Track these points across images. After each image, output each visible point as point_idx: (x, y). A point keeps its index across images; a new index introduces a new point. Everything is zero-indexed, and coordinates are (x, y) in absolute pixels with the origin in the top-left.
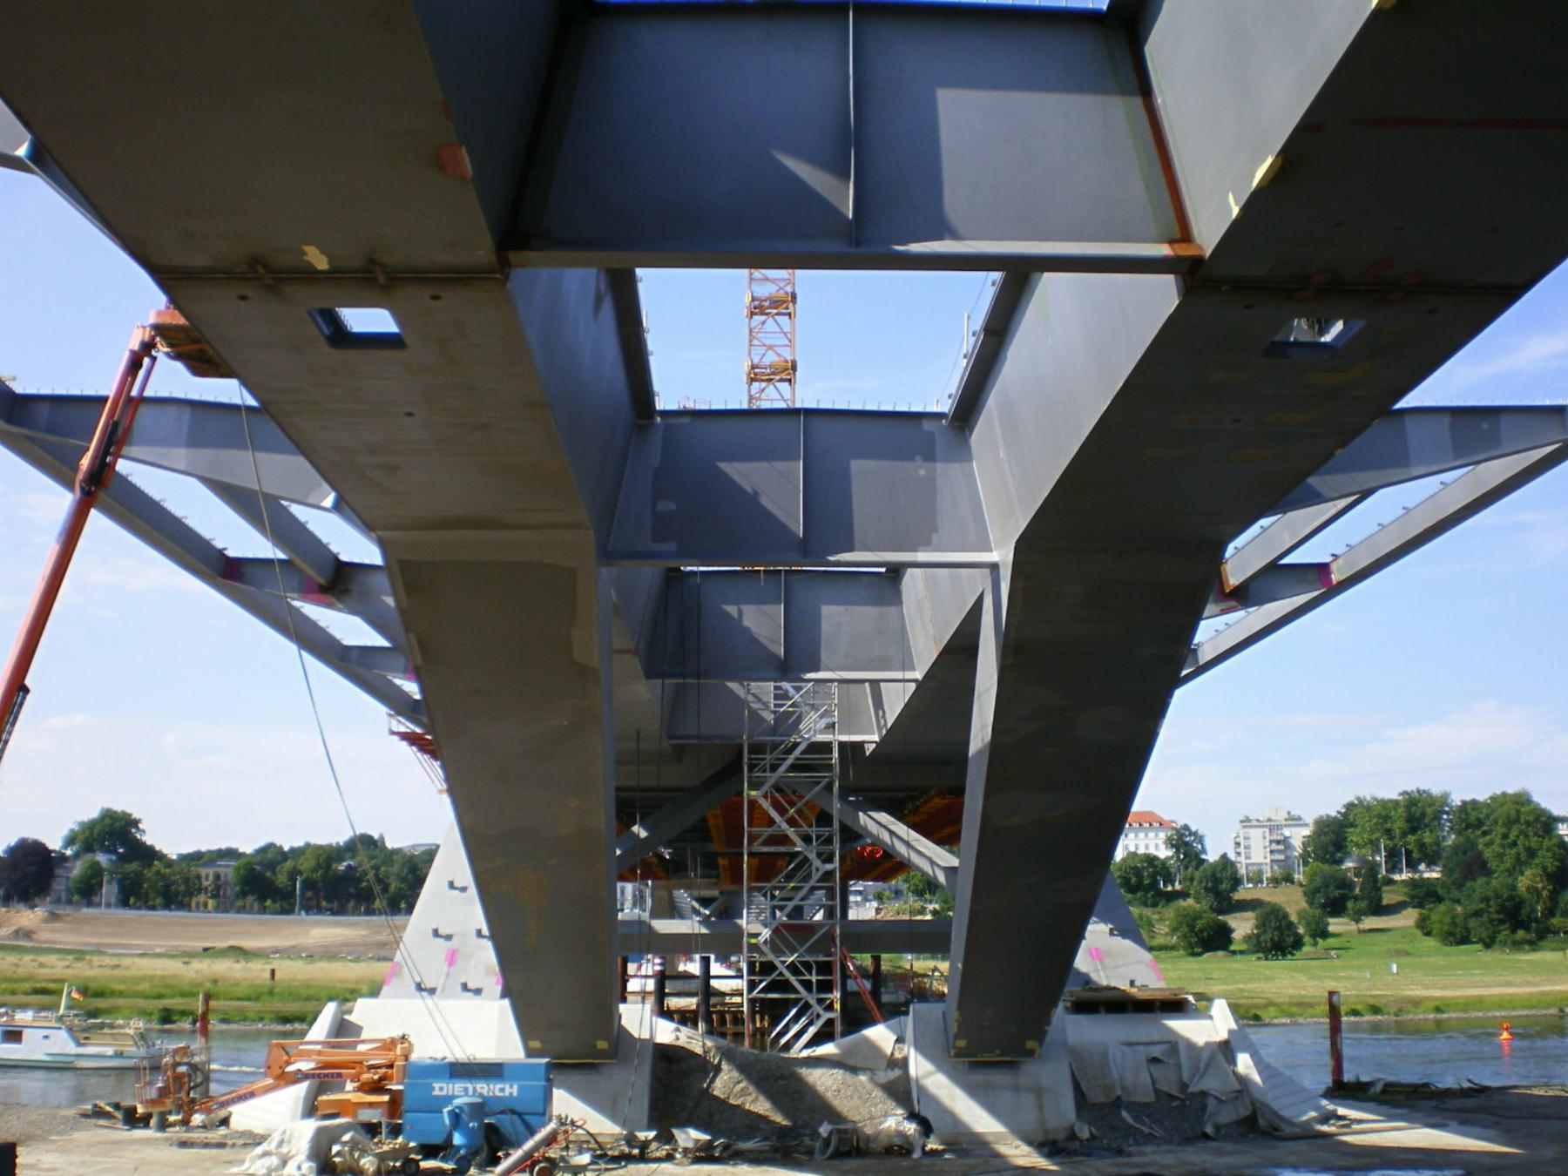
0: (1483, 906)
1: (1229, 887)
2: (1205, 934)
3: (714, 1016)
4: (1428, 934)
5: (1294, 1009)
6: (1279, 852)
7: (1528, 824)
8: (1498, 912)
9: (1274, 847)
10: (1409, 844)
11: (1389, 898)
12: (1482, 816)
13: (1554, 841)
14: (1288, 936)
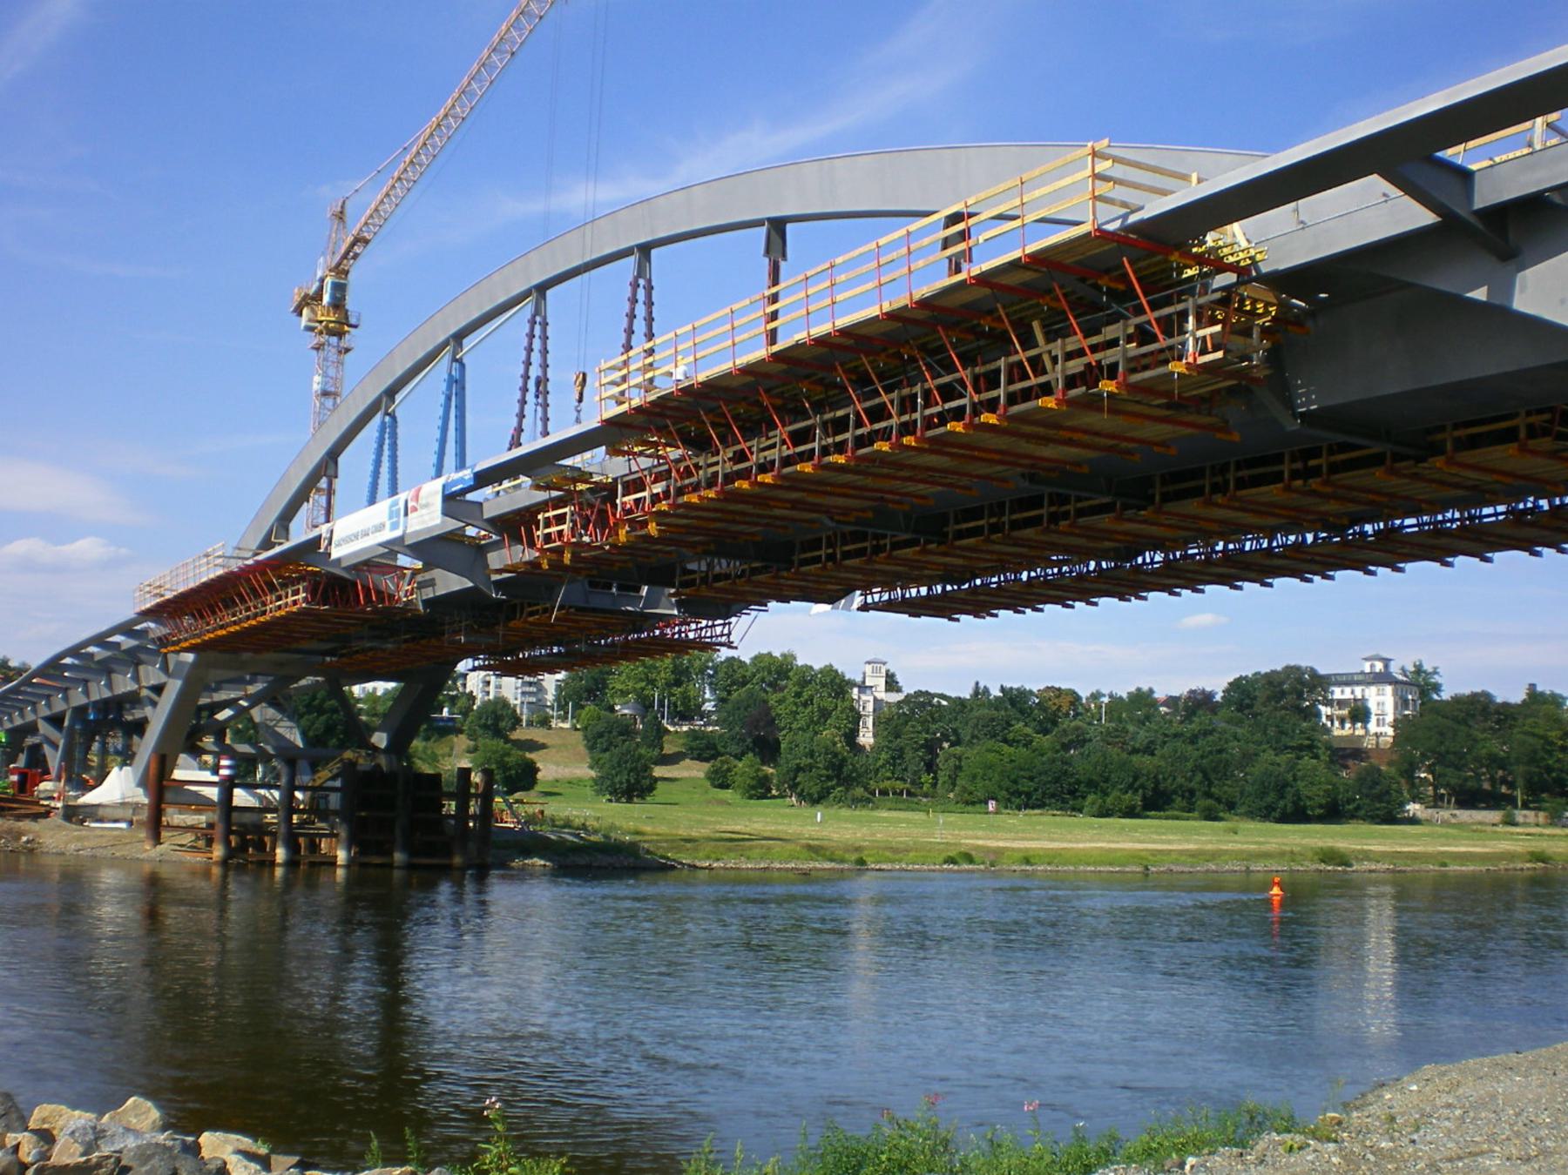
0: (809, 761)
1: (509, 724)
2: (513, 772)
3: (301, 840)
4: (724, 786)
5: (888, 854)
6: (530, 694)
7: (823, 685)
8: (826, 768)
9: (527, 689)
10: (674, 695)
11: (669, 749)
12: (748, 674)
13: (847, 704)
14: (644, 778)
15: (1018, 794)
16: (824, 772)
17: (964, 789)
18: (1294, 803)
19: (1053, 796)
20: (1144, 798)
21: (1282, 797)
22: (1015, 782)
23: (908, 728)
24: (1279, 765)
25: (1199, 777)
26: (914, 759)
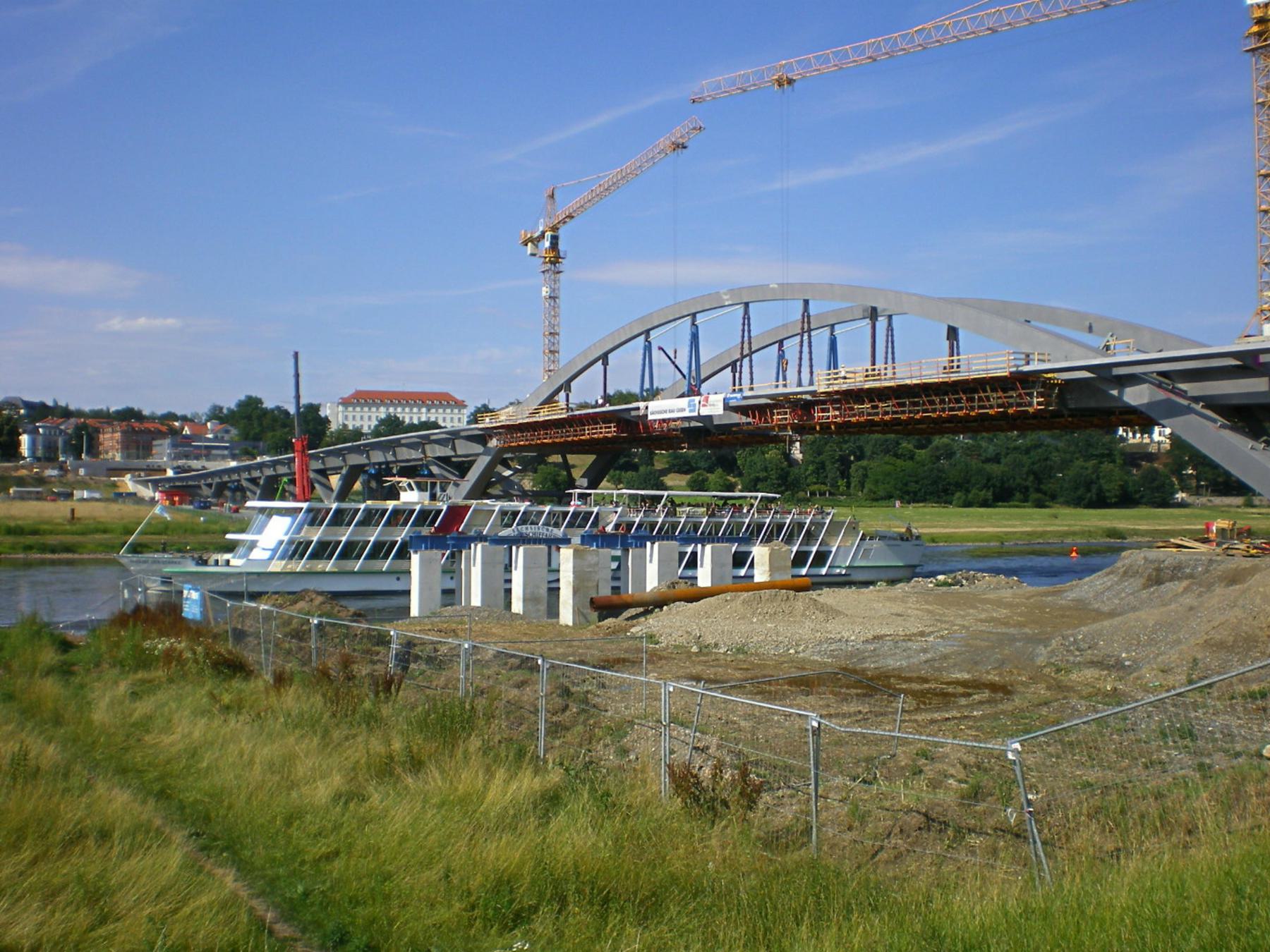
0: (765, 474)
8: (777, 479)
15: (908, 493)
16: (775, 481)
17: (871, 491)
18: (1097, 494)
19: (931, 493)
20: (994, 494)
21: (1089, 490)
22: (906, 484)
23: (828, 448)
24: (1087, 468)
25: (1031, 478)
26: (832, 470)
